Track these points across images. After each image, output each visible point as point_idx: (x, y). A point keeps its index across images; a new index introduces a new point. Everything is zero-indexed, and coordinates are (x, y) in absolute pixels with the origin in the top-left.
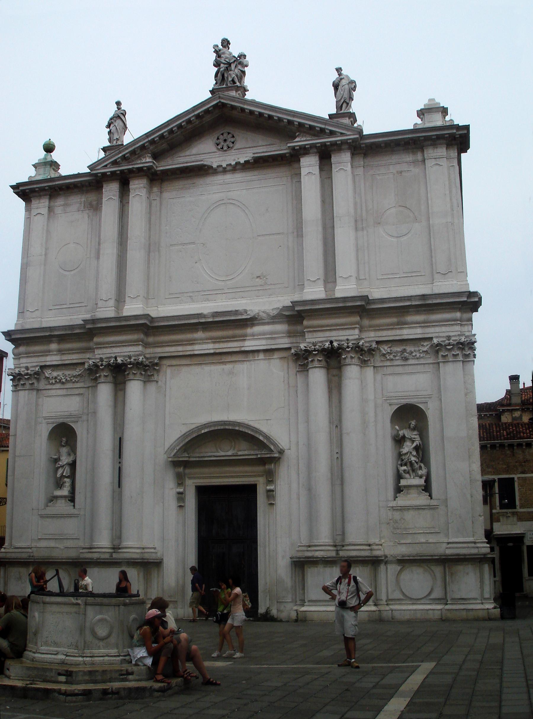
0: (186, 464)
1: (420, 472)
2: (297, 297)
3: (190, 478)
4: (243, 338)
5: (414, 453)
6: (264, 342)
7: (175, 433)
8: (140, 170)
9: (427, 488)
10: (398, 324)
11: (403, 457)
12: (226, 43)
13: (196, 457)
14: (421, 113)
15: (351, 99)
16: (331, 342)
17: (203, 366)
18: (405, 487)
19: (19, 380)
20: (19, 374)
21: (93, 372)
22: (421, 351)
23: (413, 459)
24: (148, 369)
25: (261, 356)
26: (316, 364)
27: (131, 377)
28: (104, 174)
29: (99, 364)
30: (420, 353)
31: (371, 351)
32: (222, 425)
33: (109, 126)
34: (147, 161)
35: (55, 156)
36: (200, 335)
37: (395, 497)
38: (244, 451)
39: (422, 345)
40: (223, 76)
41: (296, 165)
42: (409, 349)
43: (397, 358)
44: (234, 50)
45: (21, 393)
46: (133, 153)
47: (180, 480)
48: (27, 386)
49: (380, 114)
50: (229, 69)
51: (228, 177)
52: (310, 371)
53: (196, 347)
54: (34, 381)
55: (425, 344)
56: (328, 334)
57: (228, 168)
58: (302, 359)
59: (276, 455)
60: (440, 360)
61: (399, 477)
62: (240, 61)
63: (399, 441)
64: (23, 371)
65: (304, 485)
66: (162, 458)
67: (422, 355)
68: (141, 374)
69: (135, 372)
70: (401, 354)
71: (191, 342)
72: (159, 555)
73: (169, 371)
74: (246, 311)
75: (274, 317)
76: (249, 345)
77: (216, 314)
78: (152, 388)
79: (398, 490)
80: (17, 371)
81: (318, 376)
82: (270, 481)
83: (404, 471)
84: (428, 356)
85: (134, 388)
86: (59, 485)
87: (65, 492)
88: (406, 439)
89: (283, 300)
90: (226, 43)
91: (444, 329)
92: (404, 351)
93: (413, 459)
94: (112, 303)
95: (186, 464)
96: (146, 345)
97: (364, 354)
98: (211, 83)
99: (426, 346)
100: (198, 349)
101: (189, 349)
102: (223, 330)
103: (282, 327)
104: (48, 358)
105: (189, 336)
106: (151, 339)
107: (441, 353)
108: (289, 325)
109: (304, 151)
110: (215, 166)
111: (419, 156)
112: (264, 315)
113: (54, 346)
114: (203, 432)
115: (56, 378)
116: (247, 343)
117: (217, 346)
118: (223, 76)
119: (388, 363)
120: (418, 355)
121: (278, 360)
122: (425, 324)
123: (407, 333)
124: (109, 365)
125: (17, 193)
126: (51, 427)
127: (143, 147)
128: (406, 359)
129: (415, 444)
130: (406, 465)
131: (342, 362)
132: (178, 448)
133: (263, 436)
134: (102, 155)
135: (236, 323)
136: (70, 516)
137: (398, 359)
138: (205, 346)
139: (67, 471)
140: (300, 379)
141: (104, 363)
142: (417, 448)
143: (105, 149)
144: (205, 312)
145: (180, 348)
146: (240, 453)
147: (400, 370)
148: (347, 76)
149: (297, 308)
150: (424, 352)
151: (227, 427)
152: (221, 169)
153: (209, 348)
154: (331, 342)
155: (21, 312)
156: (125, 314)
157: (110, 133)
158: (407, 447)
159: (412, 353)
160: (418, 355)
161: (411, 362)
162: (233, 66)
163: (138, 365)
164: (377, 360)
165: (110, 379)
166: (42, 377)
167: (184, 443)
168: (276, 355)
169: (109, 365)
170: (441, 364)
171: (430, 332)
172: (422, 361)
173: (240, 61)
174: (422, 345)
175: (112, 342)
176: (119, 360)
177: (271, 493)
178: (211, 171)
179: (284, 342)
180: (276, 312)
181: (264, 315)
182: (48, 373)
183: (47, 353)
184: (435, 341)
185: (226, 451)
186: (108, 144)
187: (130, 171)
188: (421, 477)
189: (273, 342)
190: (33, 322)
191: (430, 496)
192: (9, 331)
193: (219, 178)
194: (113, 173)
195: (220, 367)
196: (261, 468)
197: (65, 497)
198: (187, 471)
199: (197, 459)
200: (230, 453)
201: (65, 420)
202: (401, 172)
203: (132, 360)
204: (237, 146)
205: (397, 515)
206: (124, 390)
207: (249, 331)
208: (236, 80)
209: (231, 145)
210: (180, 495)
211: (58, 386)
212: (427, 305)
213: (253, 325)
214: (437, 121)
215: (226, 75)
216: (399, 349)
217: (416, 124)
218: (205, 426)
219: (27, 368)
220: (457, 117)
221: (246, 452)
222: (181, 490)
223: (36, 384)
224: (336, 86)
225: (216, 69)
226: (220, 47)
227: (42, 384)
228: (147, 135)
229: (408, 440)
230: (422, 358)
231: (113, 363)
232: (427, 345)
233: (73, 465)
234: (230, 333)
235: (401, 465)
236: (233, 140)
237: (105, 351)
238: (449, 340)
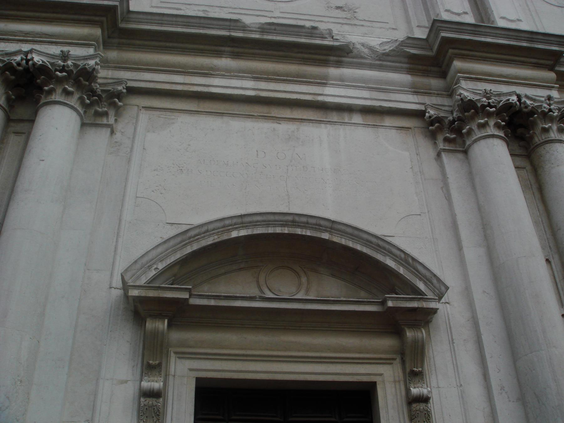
0: (178, 313)
3: (182, 355)
4: (323, 82)
6: (365, 94)
13: (209, 297)
17: (226, 119)
25: (357, 118)
26: (491, 130)
27: (57, 96)
32: (284, 224)
47: (152, 357)
58: (451, 130)
65: (502, 388)
66: (105, 292)
68: (81, 100)
69: (70, 89)
73: (144, 116)
75: (385, 56)
78: (98, 138)
81: (494, 153)
82: (415, 375)
100: (218, 85)
101: (198, 83)
112: (366, 51)
114: (234, 234)
116: (328, 90)
121: (394, 131)
131: (537, 140)
132: (161, 266)
133: (395, 258)
140: (452, 163)
151: (299, 231)
153: (246, 87)
167: (178, 255)
177: (422, 406)
180: (388, 48)
181: (366, 51)
189: (382, 96)
195: (267, 126)
196: (386, 343)
198: (176, 336)
199: (212, 303)
203: (70, 63)
207: (333, 71)
210: (151, 401)
213: (339, 64)
222: (157, 385)
231: (19, 64)
234: (293, 68)
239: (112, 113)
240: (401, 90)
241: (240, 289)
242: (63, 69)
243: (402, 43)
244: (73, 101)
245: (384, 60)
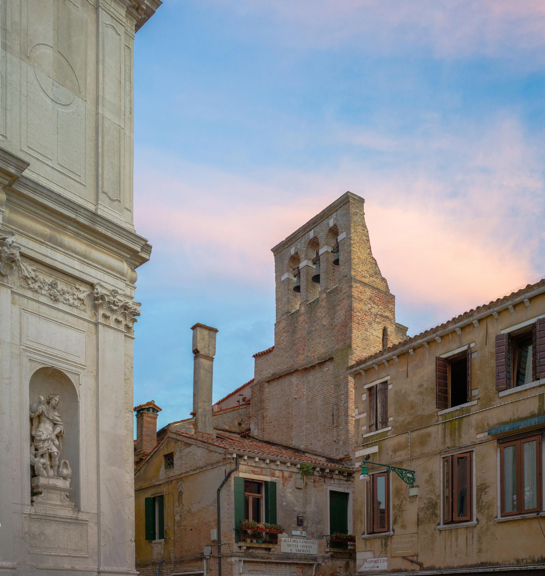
5: (57, 442)
11: (41, 445)
22: (75, 297)
23: (55, 450)
30: (74, 299)
37: (32, 501)
39: (78, 289)
42: (61, 286)
43: (44, 292)
55: (82, 288)
63: (35, 419)
67: (76, 304)
70: (49, 289)
83: (44, 464)
84: (82, 307)
88: (44, 419)
92: (53, 286)
93: (55, 450)
107: (101, 312)
120: (72, 301)
128: (56, 300)
129: (58, 430)
130: (42, 456)
137: (45, 295)
147: (44, 310)
150: (79, 299)
158: (46, 430)
159: (64, 294)
160: (72, 301)
161: (60, 306)
170: (100, 327)
172: (75, 311)
174: (78, 289)
205: (36, 528)
229: (48, 422)
230: (76, 307)
232: (84, 292)
235: (35, 456)
238: (114, 297)
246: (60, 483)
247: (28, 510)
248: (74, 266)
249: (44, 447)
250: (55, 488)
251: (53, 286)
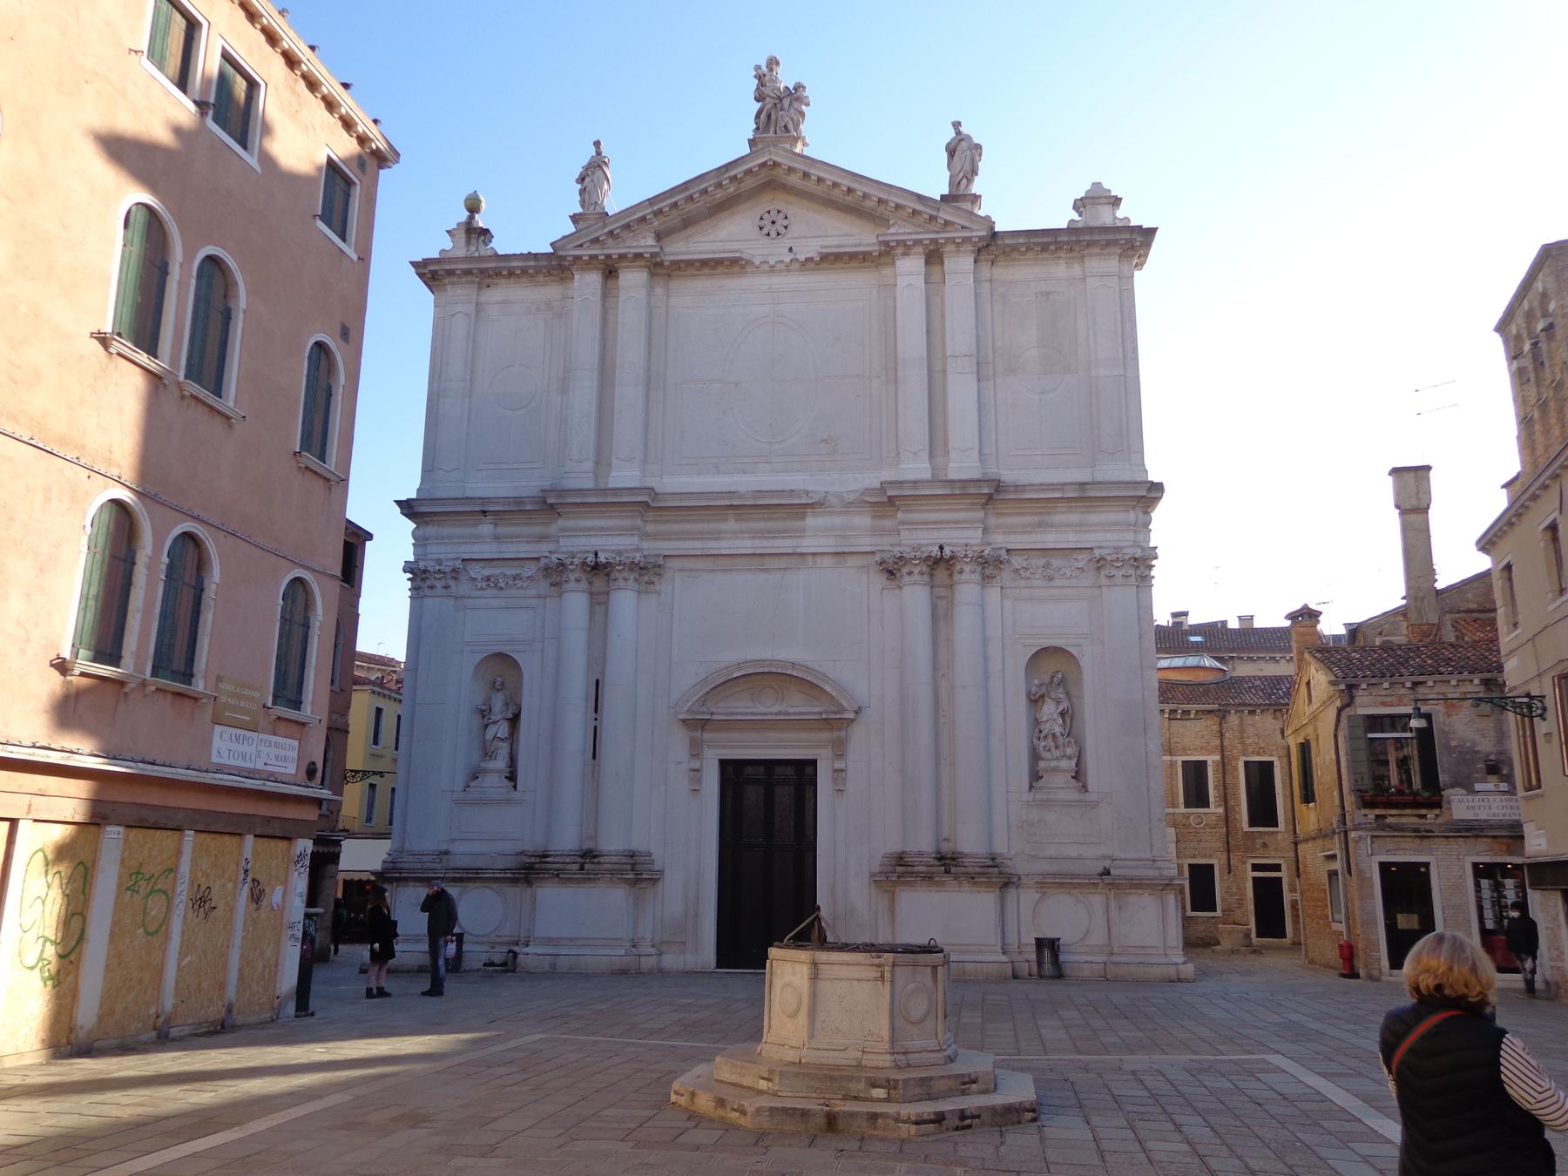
0: (704, 724)
1: (1069, 751)
2: (888, 475)
3: (710, 747)
4: (800, 533)
6: (832, 541)
7: (688, 677)
8: (638, 256)
9: (1078, 775)
10: (1039, 525)
12: (773, 63)
14: (1079, 205)
15: (974, 172)
16: (941, 548)
18: (1047, 770)
19: (423, 580)
20: (425, 571)
21: (555, 572)
23: (1058, 730)
24: (646, 571)
25: (828, 561)
26: (916, 577)
27: (621, 583)
28: (577, 258)
29: (568, 561)
31: (998, 562)
33: (581, 180)
34: (645, 242)
35: (481, 221)
36: (731, 525)
37: (1031, 787)
38: (798, 705)
40: (769, 116)
41: (887, 271)
42: (1056, 562)
44: (786, 78)
45: (428, 602)
46: (627, 227)
47: (696, 749)
48: (440, 591)
49: (1020, 199)
50: (778, 108)
51: (777, 281)
52: (906, 589)
53: (724, 543)
54: (452, 583)
56: (935, 534)
57: (782, 266)
59: (852, 716)
60: (1104, 581)
61: (1035, 756)
62: (795, 95)
63: (1035, 701)
64: (431, 566)
71: (717, 536)
72: (656, 867)
74: (807, 493)
76: (809, 544)
77: (759, 493)
79: (1035, 776)
80: (422, 565)
85: (625, 600)
86: (488, 754)
87: (500, 763)
89: (872, 480)
90: (773, 63)
91: (1109, 536)
92: (1047, 566)
94: (589, 466)
95: (704, 724)
96: (645, 536)
97: (990, 565)
98: (748, 129)
99: (1083, 560)
100: (725, 546)
101: (713, 546)
102: (769, 519)
103: (863, 521)
104: (476, 548)
105: (714, 526)
106: (650, 528)
108: (874, 517)
109: (907, 248)
110: (757, 261)
111: (1076, 270)
113: (486, 528)
115: (488, 579)
117: (757, 543)
118: (769, 116)
119: (1023, 583)
122: (1079, 527)
123: (1051, 539)
124: (584, 564)
125: (421, 276)
126: (479, 657)
127: (643, 219)
128: (1051, 579)
131: (956, 577)
134: (570, 228)
135: (794, 509)
136: (508, 802)
138: (739, 543)
139: (503, 730)
141: (576, 561)
142: (1062, 714)
143: (575, 218)
144: (743, 489)
145: (698, 544)
146: (790, 710)
148: (969, 137)
149: (891, 493)
152: (766, 267)
153: (746, 545)
154: (941, 548)
155: (428, 469)
156: (611, 485)
157: (582, 192)
158: (1049, 709)
161: (1056, 583)
162: (786, 102)
163: (633, 566)
164: (1006, 575)
165: (584, 585)
166: (463, 577)
168: (852, 561)
169: (584, 564)
171: (1089, 539)
173: (795, 95)
175: (590, 529)
176: (602, 558)
178: (749, 269)
179: (865, 543)
180: (852, 497)
182: (477, 571)
183: (476, 539)
184: (1097, 553)
185: (769, 707)
186: (579, 210)
187: (622, 257)
188: (1069, 758)
190: (448, 489)
191: (1085, 788)
192: (408, 500)
193: (762, 282)
194: (593, 257)
196: (825, 735)
197: (499, 771)
198: (706, 736)
200: (775, 709)
201: (504, 649)
202: (1048, 293)
204: (792, 231)
206: (606, 604)
207: (811, 521)
208: (790, 126)
209: (782, 230)
211: (490, 592)
212: (1084, 496)
214: (1104, 217)
215: (773, 117)
216: (1041, 562)
217: (1072, 221)
218: (739, 665)
219: (439, 562)
220: (1133, 212)
221: (802, 709)
222: (697, 766)
223: (453, 589)
224: (951, 151)
225: (759, 105)
226: (764, 69)
227: (463, 588)
228: (652, 201)
233: (514, 720)
236: (786, 223)
237: (575, 541)
239: (656, 579)
240: (862, 530)
241: (742, 706)
242: (620, 564)
243: (863, 494)
244: (631, 583)
245: (851, 505)
246: (1064, 764)
247: (1030, 796)
248: (1070, 539)
249: (1046, 728)
250: (1056, 769)
251: (1047, 566)
